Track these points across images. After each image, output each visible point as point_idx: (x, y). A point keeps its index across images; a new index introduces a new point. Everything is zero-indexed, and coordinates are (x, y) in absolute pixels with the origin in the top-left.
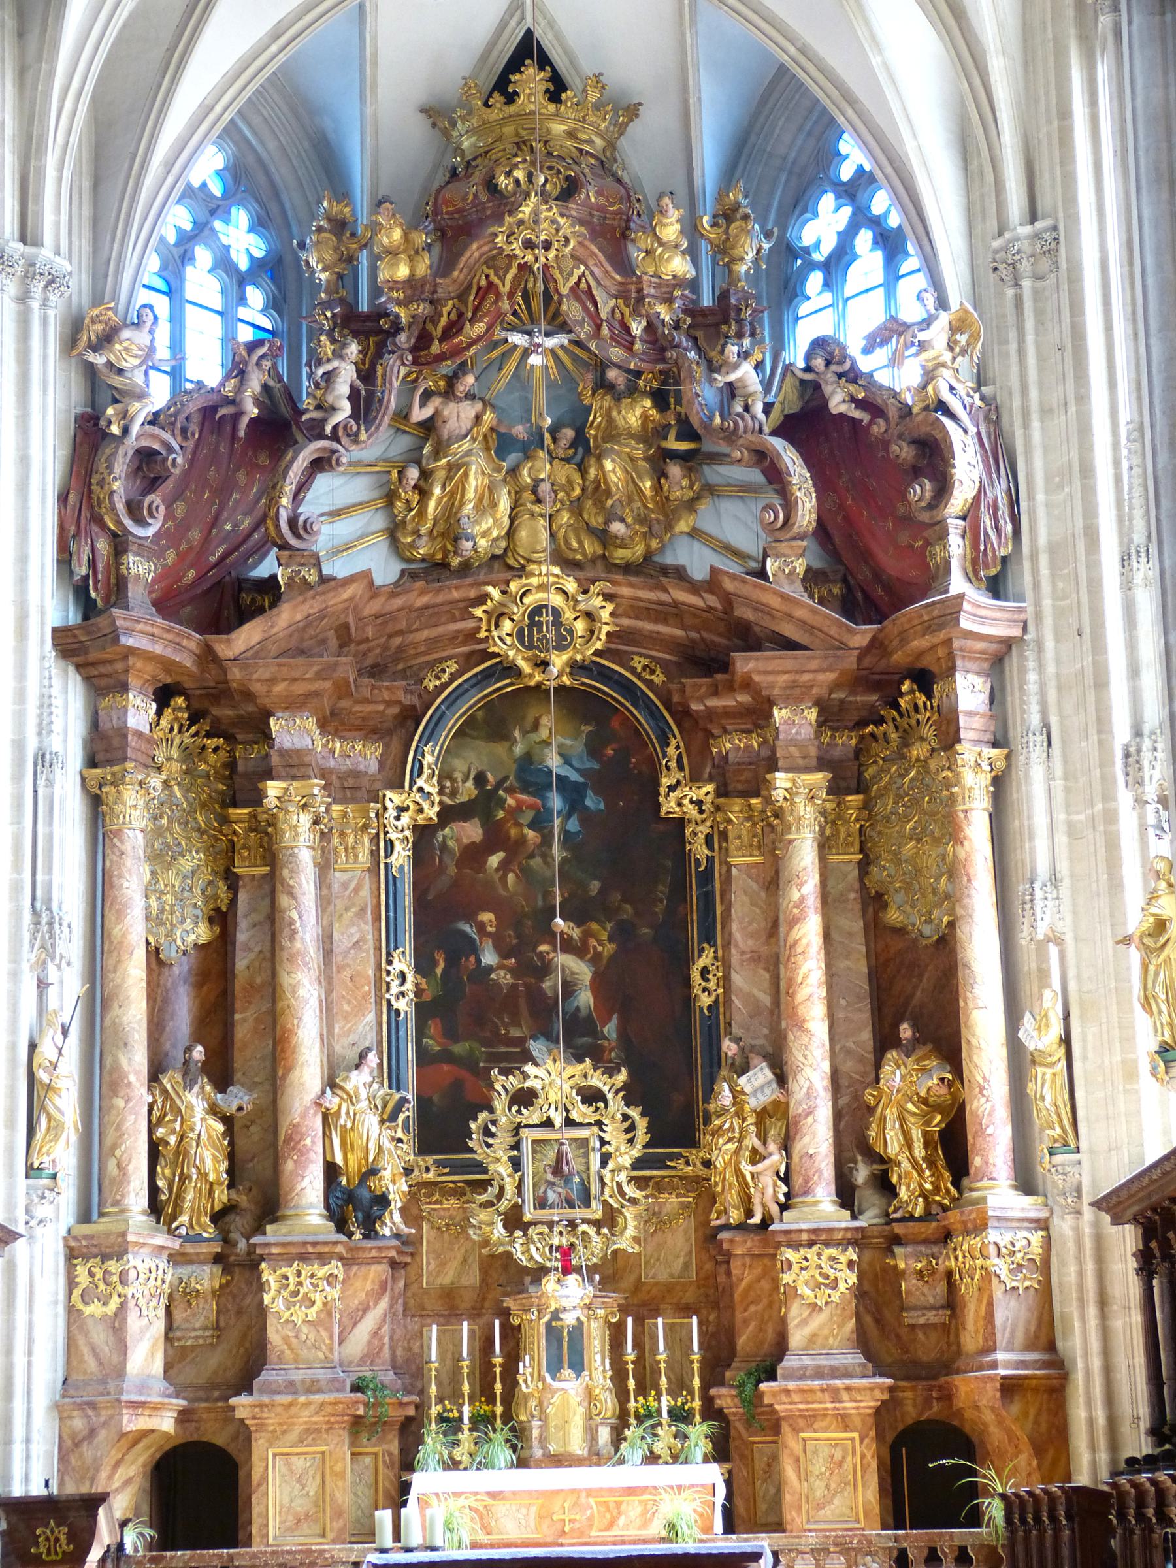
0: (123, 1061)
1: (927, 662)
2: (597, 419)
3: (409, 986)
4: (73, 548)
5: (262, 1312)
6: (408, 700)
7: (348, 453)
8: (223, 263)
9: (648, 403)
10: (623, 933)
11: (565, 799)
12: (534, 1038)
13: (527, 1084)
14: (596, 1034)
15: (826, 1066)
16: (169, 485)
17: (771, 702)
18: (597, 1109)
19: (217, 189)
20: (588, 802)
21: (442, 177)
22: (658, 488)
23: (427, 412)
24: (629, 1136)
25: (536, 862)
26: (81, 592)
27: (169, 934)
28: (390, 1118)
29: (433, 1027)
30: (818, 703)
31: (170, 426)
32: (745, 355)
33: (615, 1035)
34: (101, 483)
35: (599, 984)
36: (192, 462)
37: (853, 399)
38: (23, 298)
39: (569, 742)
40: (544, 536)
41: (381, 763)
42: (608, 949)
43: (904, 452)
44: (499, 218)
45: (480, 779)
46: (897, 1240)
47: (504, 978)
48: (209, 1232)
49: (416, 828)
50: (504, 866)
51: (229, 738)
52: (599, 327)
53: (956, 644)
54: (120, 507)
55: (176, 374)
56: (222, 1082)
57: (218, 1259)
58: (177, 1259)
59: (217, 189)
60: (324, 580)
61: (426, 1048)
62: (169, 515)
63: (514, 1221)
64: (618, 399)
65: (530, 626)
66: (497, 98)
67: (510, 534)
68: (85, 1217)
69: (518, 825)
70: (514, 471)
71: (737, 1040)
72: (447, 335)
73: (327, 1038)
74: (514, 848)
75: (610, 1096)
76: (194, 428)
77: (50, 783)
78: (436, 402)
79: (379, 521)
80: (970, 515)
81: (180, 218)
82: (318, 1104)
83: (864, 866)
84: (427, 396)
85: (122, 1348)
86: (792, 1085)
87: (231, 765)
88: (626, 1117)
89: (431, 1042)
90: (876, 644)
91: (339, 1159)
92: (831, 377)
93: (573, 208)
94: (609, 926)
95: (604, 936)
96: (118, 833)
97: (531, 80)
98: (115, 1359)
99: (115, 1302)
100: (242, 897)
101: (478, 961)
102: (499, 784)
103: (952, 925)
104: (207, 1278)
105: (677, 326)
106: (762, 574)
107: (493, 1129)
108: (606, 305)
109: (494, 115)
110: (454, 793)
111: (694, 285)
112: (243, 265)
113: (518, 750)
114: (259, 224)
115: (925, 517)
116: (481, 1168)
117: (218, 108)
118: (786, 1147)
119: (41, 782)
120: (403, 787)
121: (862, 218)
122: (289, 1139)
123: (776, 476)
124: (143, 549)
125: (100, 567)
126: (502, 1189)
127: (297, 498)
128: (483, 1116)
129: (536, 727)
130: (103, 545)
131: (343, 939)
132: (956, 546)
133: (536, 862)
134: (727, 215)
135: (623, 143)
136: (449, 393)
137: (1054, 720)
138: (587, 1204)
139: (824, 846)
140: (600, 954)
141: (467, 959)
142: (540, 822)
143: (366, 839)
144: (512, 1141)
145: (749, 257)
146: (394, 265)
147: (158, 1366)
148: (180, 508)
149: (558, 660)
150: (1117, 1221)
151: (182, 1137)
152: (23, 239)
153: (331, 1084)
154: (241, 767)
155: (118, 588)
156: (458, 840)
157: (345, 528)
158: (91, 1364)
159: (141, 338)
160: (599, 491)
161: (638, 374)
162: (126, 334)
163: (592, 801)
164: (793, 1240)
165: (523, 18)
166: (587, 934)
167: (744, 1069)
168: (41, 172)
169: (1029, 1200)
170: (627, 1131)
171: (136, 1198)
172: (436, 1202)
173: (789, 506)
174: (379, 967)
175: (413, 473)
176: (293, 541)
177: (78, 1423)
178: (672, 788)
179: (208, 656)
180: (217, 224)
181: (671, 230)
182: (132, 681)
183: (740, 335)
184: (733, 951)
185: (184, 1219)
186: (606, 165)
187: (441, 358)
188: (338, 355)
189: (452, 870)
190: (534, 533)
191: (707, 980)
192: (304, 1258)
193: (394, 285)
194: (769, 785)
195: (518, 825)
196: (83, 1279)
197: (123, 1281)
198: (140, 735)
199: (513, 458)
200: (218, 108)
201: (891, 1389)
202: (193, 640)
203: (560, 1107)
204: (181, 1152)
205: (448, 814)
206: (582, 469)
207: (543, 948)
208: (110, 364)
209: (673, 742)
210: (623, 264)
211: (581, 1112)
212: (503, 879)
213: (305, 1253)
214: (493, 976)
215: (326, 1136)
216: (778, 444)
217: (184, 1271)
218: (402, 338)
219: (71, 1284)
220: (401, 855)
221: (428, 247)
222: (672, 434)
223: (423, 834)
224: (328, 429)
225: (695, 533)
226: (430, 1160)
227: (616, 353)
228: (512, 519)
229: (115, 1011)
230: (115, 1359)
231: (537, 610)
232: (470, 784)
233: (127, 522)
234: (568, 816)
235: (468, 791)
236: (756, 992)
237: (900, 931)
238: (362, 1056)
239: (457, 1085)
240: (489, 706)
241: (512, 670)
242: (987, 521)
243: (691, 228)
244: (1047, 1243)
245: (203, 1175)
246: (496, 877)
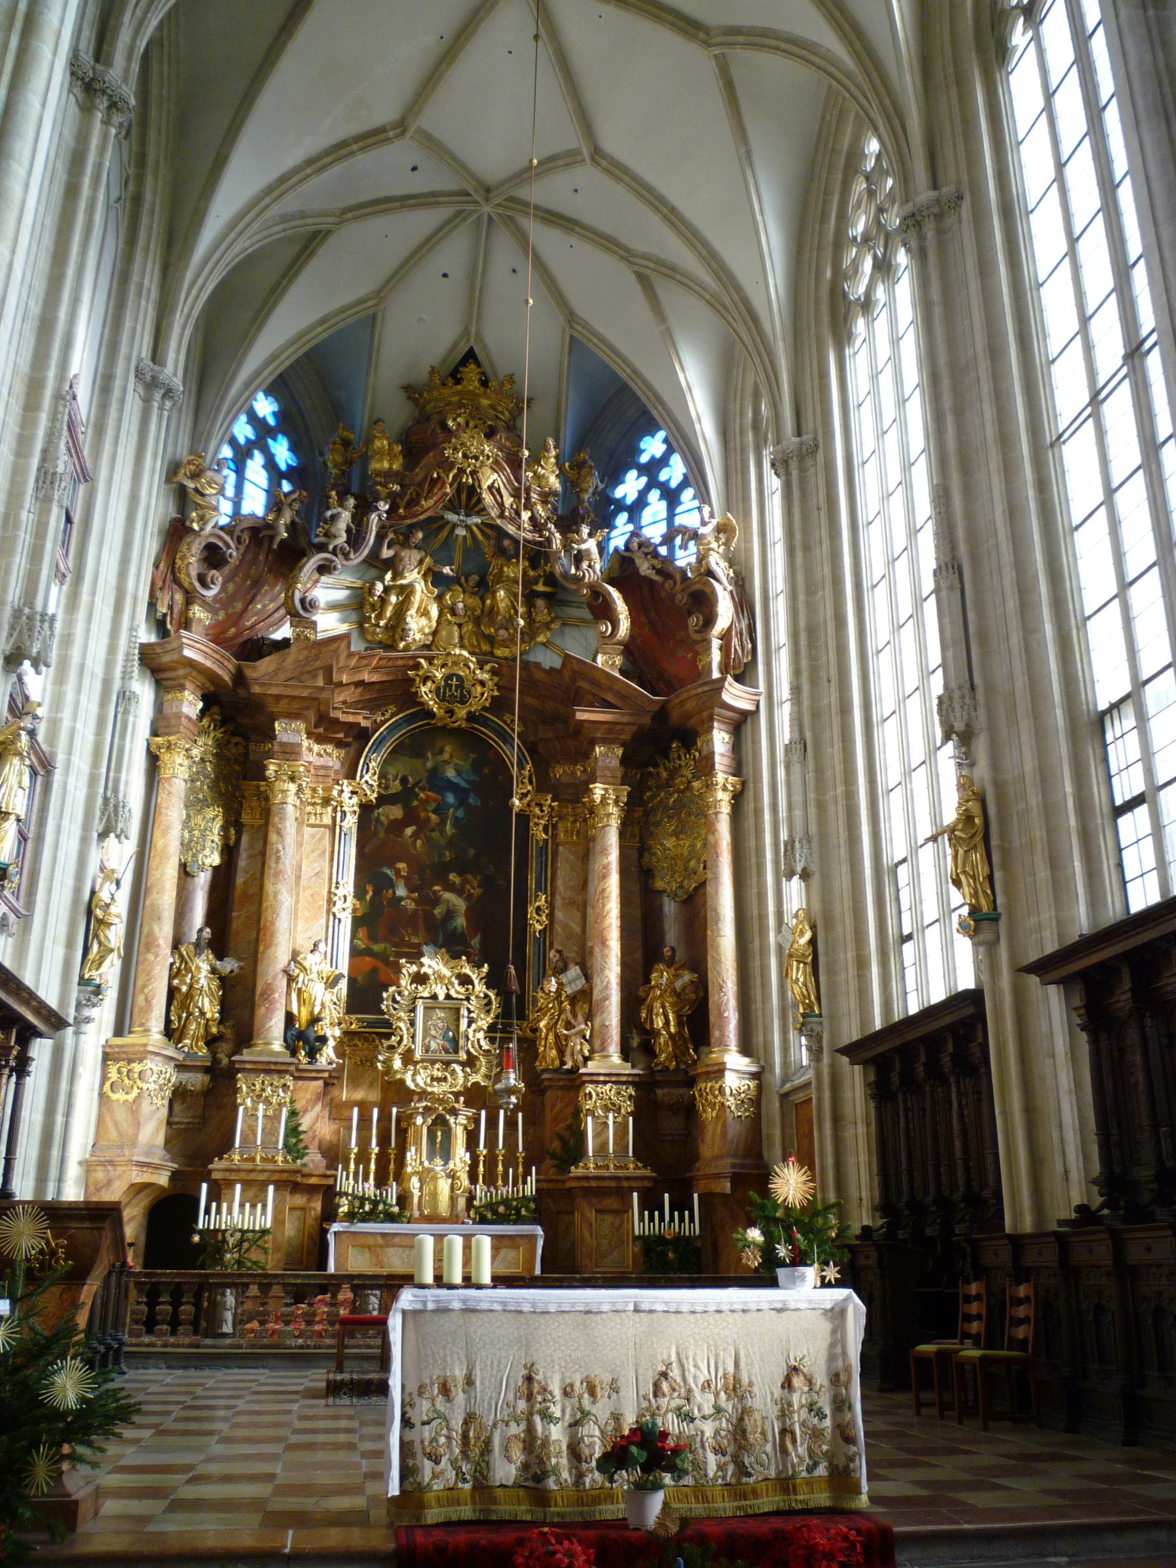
1: (692, 723)
2: (493, 570)
4: (159, 594)
11: (456, 797)
12: (427, 944)
14: (467, 945)
19: (271, 421)
20: (471, 801)
25: (435, 835)
26: (160, 626)
29: (362, 933)
33: (478, 946)
35: (469, 914)
39: (461, 763)
40: (456, 635)
41: (343, 764)
42: (477, 892)
43: (682, 599)
45: (404, 781)
46: (658, 1084)
47: (410, 905)
48: (204, 1051)
49: (361, 806)
50: (415, 835)
51: (247, 738)
52: (503, 512)
55: (237, 504)
56: (220, 956)
59: (271, 421)
62: (224, 588)
63: (408, 1058)
64: (509, 559)
65: (445, 687)
69: (426, 810)
72: (408, 506)
75: (476, 982)
85: (137, 1125)
86: (597, 981)
87: (246, 755)
88: (486, 996)
90: (662, 714)
91: (295, 1011)
92: (640, 554)
94: (479, 877)
95: (475, 884)
98: (131, 1132)
99: (136, 1091)
100: (245, 839)
101: (394, 893)
102: (416, 784)
107: (398, 998)
108: (508, 501)
109: (446, 391)
110: (387, 788)
112: (283, 467)
113: (429, 764)
114: (293, 449)
116: (388, 1024)
117: (282, 358)
118: (589, 1017)
119: (121, 709)
120: (354, 778)
121: (653, 483)
122: (264, 993)
125: (176, 610)
126: (402, 1037)
128: (392, 989)
129: (441, 751)
133: (435, 835)
136: (404, 541)
138: (456, 1052)
139: (622, 835)
143: (330, 809)
146: (381, 460)
147: (160, 1139)
149: (462, 712)
156: (387, 817)
158: (113, 1134)
160: (492, 612)
163: (472, 800)
164: (594, 1079)
165: (469, 340)
166: (464, 882)
167: (564, 969)
168: (170, 326)
170: (486, 1005)
171: (156, 1025)
174: (330, 892)
176: (301, 612)
177: (100, 1175)
178: (524, 796)
180: (270, 441)
182: (188, 685)
184: (558, 897)
185: (187, 1041)
189: (382, 835)
191: (539, 915)
193: (379, 473)
195: (426, 810)
196: (113, 1075)
198: (189, 718)
200: (282, 358)
202: (231, 664)
204: (189, 995)
205: (382, 800)
207: (436, 888)
208: (196, 490)
209: (528, 767)
211: (457, 990)
212: (414, 843)
217: (186, 1077)
219: (104, 1078)
220: (351, 822)
222: (541, 582)
223: (366, 809)
224: (331, 547)
226: (354, 1017)
227: (511, 529)
228: (438, 622)
230: (131, 1132)
232: (397, 782)
234: (457, 808)
235: (396, 786)
236: (571, 924)
238: (316, 945)
239: (374, 971)
240: (412, 736)
241: (431, 715)
242: (735, 641)
246: (410, 841)
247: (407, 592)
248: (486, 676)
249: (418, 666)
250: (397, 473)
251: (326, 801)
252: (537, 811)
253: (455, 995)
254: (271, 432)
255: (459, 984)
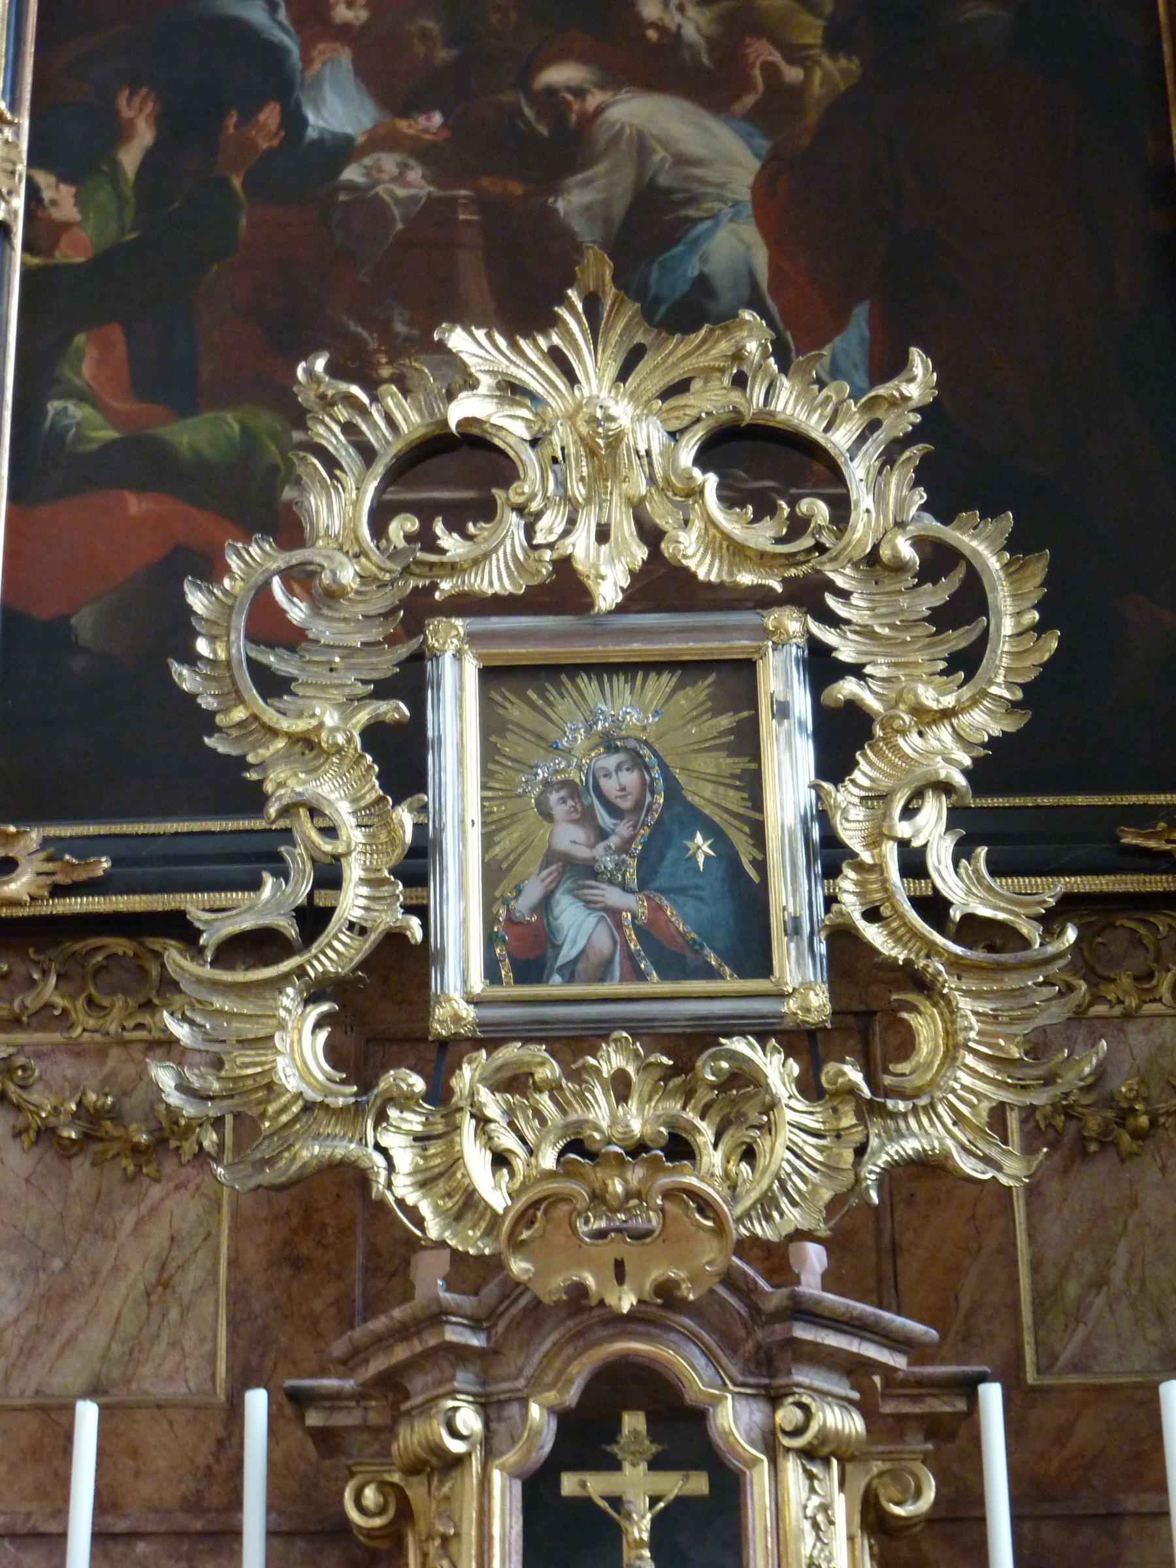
13: (459, 411)
18: (798, 526)
24: (958, 639)
61: (58, 435)
75: (857, 472)
89: (77, 412)
95: (811, 31)
101: (294, 121)
107: (297, 612)
140: (798, 91)
141: (248, 116)
144: (386, 664)
170: (942, 619)
172: (46, 1017)
203: (624, 527)
214: (352, 174)
253: (705, 569)
255: (731, 498)
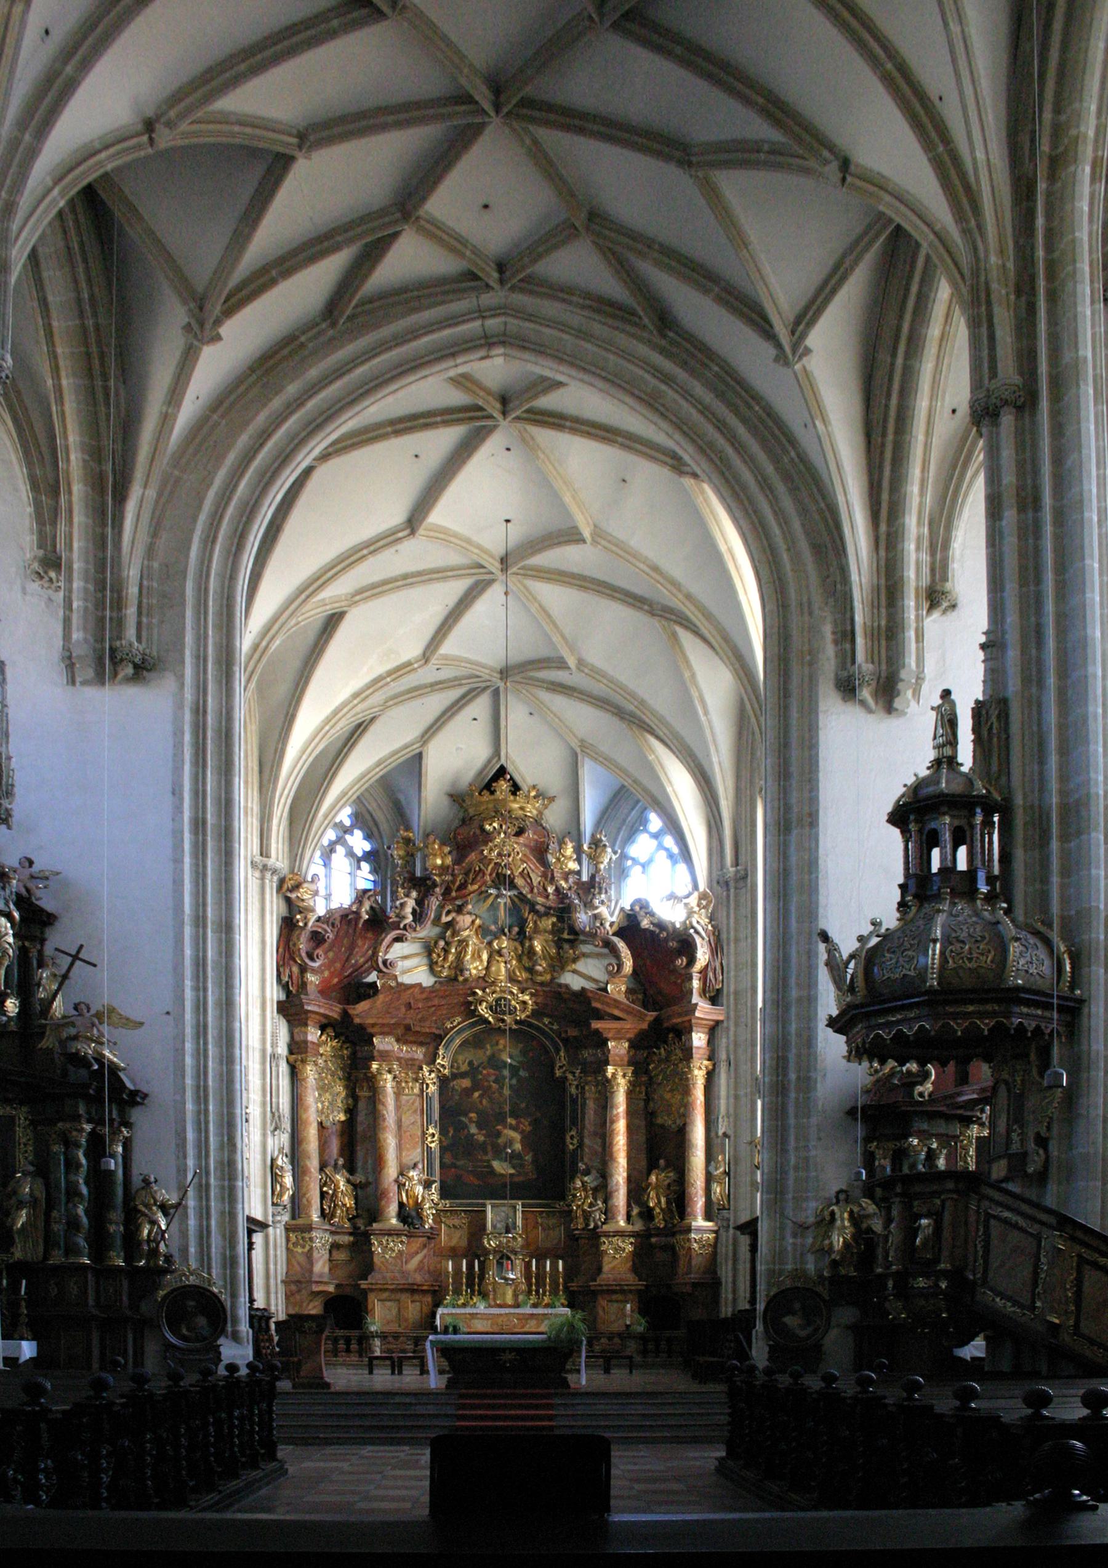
0: (308, 1163)
3: (436, 1138)
5: (372, 1253)
6: (437, 1032)
7: (409, 935)
8: (350, 853)
9: (554, 919)
10: (535, 1123)
15: (625, 1174)
16: (326, 945)
17: (607, 1040)
21: (456, 823)
22: (558, 953)
23: (449, 918)
27: (327, 1116)
28: (427, 1185)
30: (629, 1040)
31: (327, 923)
32: (602, 902)
34: (294, 945)
36: (337, 936)
37: (652, 923)
38: (262, 879)
44: (486, 844)
45: (471, 1063)
53: (693, 1021)
54: (304, 955)
57: (350, 1234)
58: (332, 1233)
60: (400, 985)
66: (485, 792)
67: (487, 968)
68: (293, 1218)
70: (490, 944)
71: (586, 1164)
73: (399, 1157)
74: (486, 1092)
76: (337, 923)
77: (277, 1066)
78: (453, 915)
79: (425, 961)
80: (704, 972)
81: (331, 835)
82: (396, 1181)
83: (647, 1101)
84: (448, 913)
93: (521, 840)
96: (304, 1080)
97: (503, 785)
103: (685, 1125)
104: (347, 1239)
105: (570, 889)
106: (605, 990)
108: (536, 879)
111: (579, 873)
115: (683, 972)
123: (614, 951)
124: (314, 971)
127: (386, 953)
130: (295, 969)
131: (407, 1119)
132: (696, 984)
134: (596, 843)
135: (546, 812)
136: (459, 910)
137: (732, 1057)
142: (499, 1080)
145: (606, 861)
148: (331, 954)
150: (743, 1234)
151: (335, 1190)
152: (261, 855)
153: (401, 1173)
154: (359, 1055)
155: (303, 985)
157: (408, 963)
159: (313, 887)
161: (550, 908)
162: (305, 885)
169: (710, 1224)
173: (620, 966)
175: (442, 943)
178: (561, 1067)
179: (345, 1014)
181: (569, 850)
183: (600, 893)
186: (537, 822)
187: (456, 899)
188: (407, 895)
190: (499, 970)
192: (390, 1235)
193: (435, 867)
194: (605, 1071)
197: (311, 1239)
199: (489, 938)
201: (646, 1286)
206: (522, 944)
210: (544, 862)
213: (391, 1233)
215: (400, 1193)
216: (616, 939)
218: (437, 890)
220: (433, 1089)
221: (450, 853)
225: (575, 972)
227: (540, 900)
228: (489, 962)
229: (304, 1146)
231: (500, 999)
233: (307, 961)
237: (662, 1126)
240: (475, 1036)
241: (486, 1021)
243: (578, 850)
244: (716, 1239)
245: (345, 1205)
247: (463, 943)
248: (527, 998)
249: (475, 994)
250: (448, 867)
251: (416, 1080)
252: (570, 1077)
254: (348, 831)
